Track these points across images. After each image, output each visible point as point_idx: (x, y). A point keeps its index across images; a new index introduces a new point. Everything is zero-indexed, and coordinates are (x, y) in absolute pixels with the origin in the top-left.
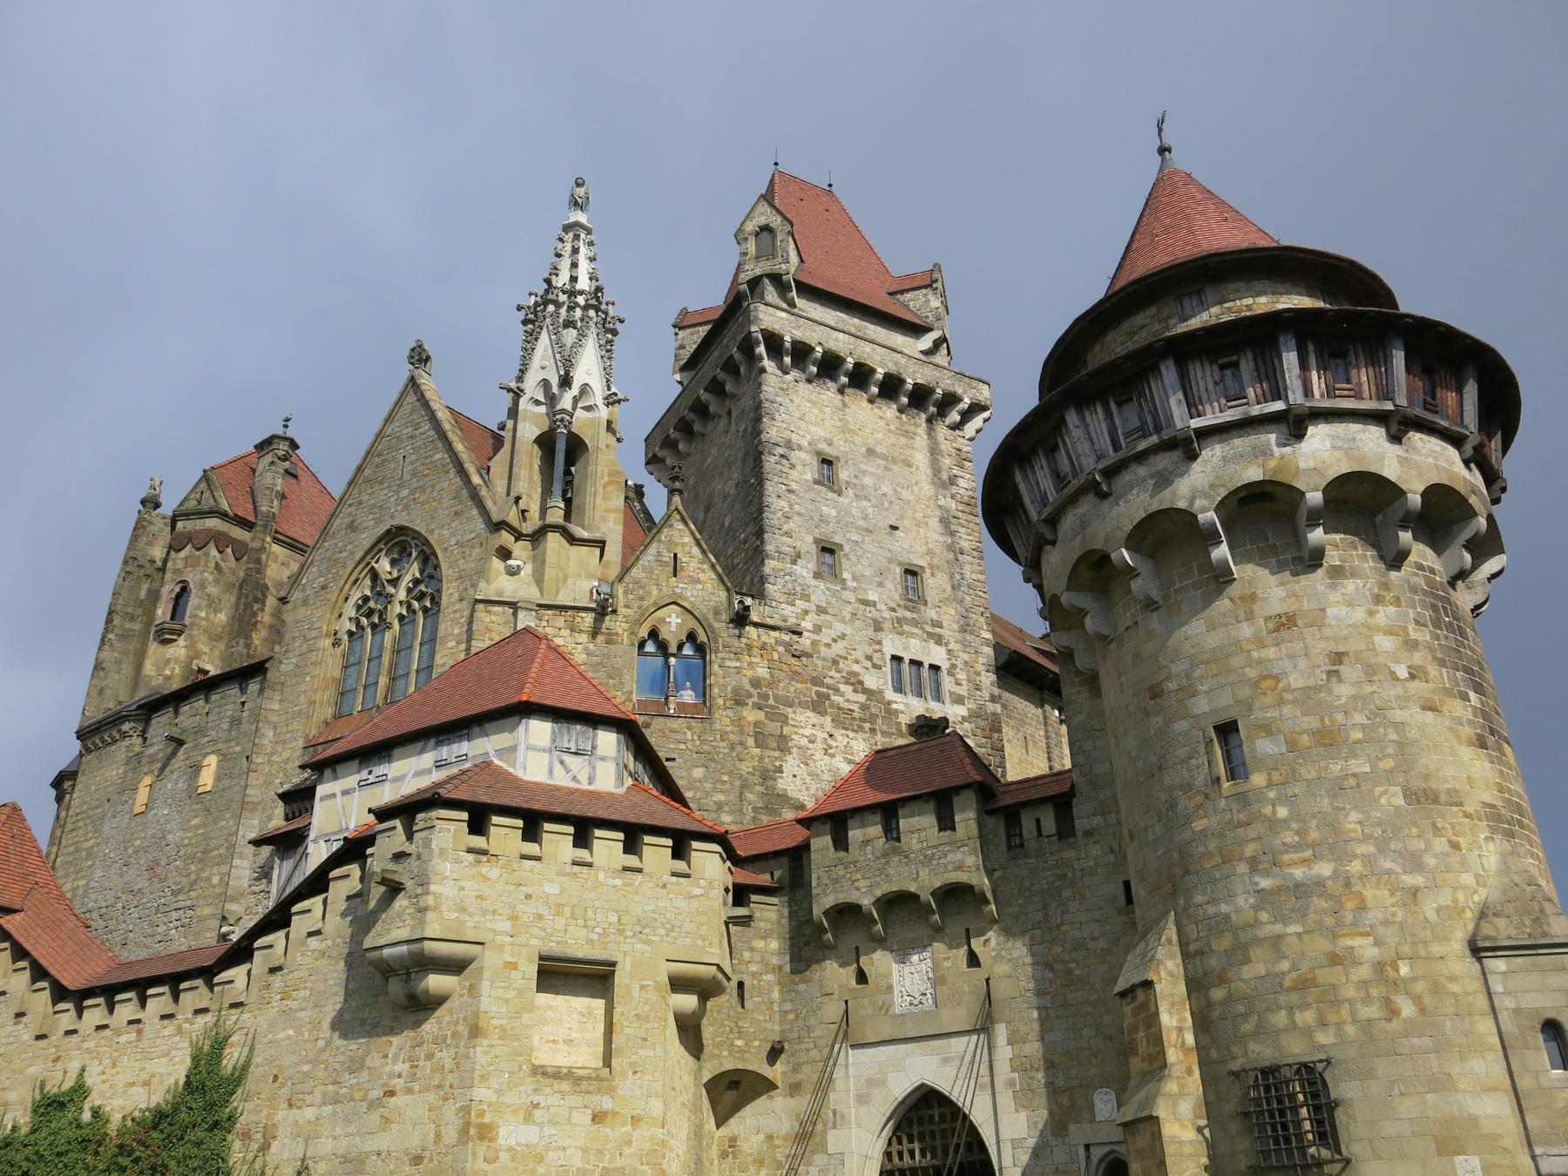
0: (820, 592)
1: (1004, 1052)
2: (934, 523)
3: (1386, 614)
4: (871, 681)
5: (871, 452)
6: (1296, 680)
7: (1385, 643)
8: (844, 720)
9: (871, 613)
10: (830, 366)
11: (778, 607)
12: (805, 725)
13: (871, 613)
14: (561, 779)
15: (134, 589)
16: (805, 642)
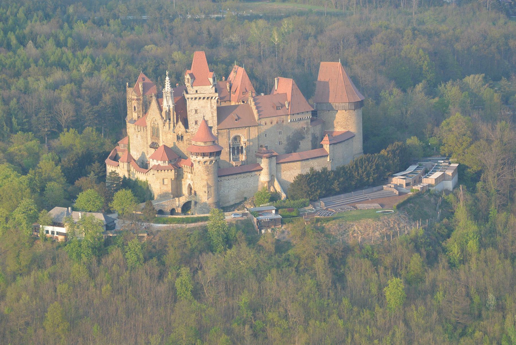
2: (210, 114)
5: (202, 107)
10: (196, 98)
11: (190, 130)
16: (194, 133)
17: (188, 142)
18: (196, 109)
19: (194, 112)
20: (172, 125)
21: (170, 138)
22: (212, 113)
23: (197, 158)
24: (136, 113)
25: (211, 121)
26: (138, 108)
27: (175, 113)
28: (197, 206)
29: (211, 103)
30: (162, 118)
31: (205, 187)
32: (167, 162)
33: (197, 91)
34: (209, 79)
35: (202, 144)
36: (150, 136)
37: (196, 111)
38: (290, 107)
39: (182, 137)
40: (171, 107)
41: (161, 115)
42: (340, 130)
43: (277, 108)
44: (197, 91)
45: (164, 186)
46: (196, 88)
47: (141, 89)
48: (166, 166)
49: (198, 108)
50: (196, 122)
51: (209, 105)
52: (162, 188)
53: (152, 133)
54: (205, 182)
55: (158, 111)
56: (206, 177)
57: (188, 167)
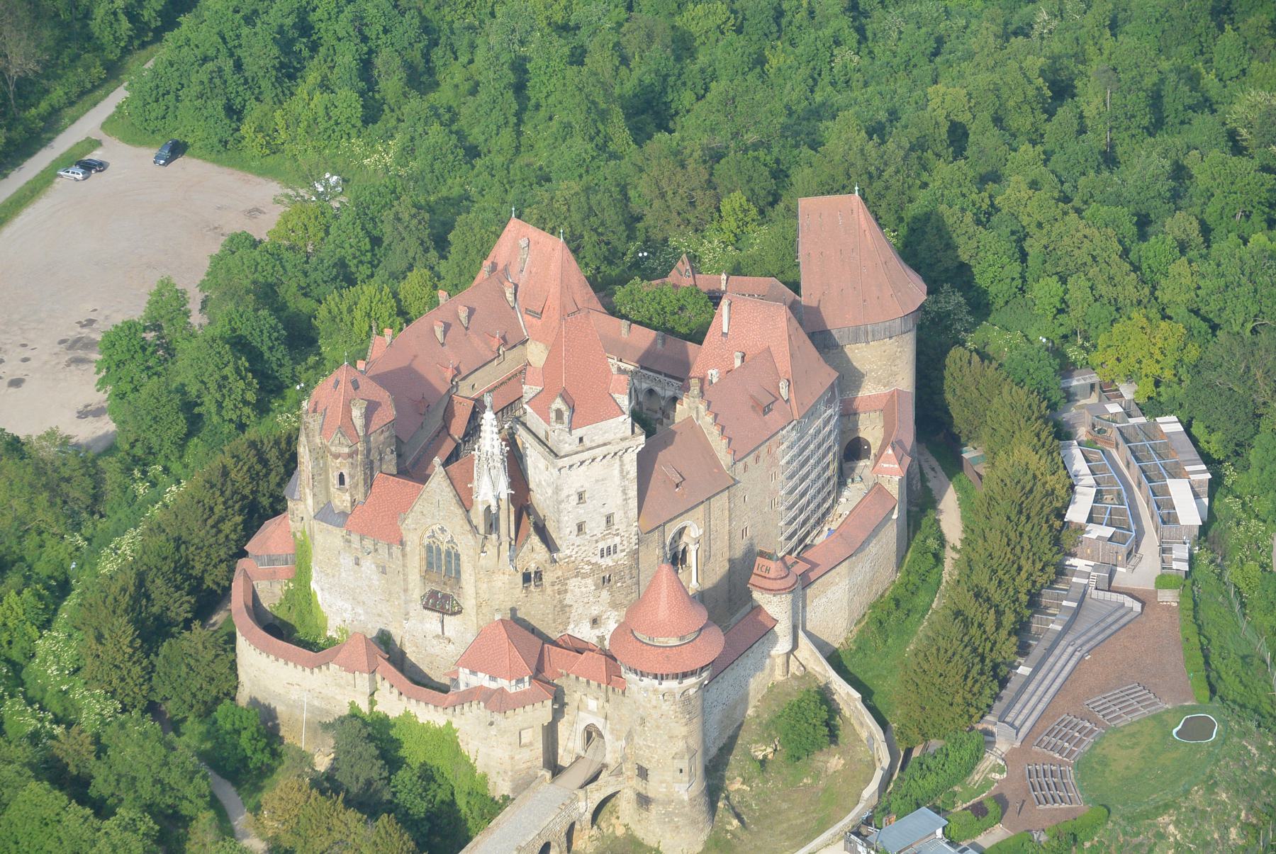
0: (578, 541)
1: (608, 726)
2: (620, 493)
3: (673, 708)
4: (593, 561)
5: (597, 481)
6: (655, 716)
7: (671, 713)
8: (585, 576)
9: (595, 538)
11: (565, 551)
12: (573, 583)
13: (595, 538)
14: (518, 690)
15: (318, 464)
16: (573, 559)
17: (556, 588)
18: (582, 490)
19: (575, 498)
20: (505, 546)
21: (500, 584)
22: (624, 492)
23: (660, 684)
24: (347, 494)
25: (621, 512)
26: (352, 477)
27: (512, 509)
28: (654, 812)
29: (622, 465)
30: (475, 529)
31: (682, 758)
32: (527, 679)
33: (581, 440)
34: (616, 396)
35: (674, 641)
36: (417, 570)
37: (580, 496)
38: (792, 395)
39: (539, 575)
40: (504, 496)
41: (470, 522)
42: (874, 393)
43: (766, 410)
44: (581, 440)
45: (524, 750)
46: (578, 433)
47: (359, 421)
48: (524, 693)
49: (587, 486)
50: (580, 528)
51: (616, 472)
52: (517, 757)
53: (424, 563)
54: (681, 745)
55: (459, 512)
56: (683, 730)
57: (594, 683)
